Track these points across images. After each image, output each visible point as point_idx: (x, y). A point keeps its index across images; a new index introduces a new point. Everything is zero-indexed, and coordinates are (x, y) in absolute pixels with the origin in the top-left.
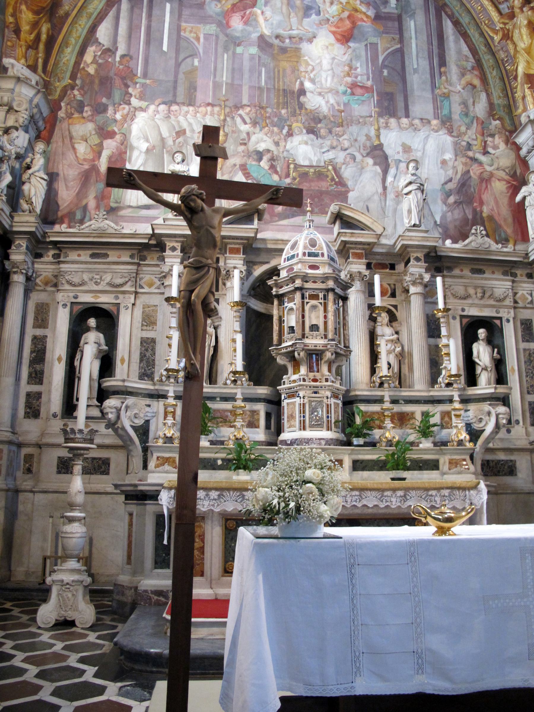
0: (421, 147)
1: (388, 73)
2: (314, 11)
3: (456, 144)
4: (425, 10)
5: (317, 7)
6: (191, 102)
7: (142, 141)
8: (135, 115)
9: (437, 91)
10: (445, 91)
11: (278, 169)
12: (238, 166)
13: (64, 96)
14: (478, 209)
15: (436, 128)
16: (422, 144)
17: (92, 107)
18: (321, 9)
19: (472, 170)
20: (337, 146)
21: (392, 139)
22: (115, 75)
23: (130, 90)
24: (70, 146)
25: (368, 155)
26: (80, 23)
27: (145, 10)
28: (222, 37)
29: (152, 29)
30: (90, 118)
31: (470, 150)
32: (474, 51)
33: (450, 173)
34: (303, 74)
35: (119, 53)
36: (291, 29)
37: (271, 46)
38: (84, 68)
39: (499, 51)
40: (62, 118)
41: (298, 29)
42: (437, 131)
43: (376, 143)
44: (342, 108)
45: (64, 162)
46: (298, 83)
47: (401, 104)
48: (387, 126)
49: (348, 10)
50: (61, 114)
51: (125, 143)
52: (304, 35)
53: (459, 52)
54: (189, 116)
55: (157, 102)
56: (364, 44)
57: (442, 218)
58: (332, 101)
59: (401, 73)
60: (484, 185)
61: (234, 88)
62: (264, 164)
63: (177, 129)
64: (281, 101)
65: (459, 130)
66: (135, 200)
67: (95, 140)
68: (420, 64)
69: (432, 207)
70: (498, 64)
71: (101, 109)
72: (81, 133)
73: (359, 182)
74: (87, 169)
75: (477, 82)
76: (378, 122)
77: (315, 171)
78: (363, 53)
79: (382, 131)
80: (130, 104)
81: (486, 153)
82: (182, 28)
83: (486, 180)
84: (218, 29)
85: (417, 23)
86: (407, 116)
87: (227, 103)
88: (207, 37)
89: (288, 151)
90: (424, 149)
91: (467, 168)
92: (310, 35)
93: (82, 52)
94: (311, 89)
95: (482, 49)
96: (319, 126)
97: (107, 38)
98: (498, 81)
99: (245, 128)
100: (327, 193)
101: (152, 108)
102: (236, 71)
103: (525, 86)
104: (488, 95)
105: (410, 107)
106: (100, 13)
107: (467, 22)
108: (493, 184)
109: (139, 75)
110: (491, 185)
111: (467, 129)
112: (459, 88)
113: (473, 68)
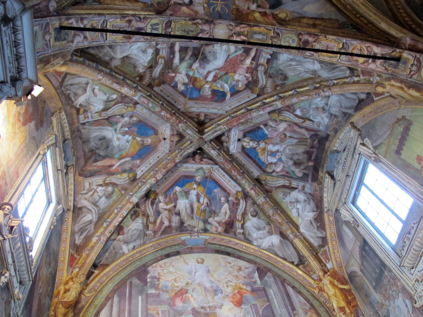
26: (90, 311)
28: (172, 312)
29: (132, 311)
32: (307, 300)
36: (209, 303)
39: (319, 297)
41: (212, 302)
53: (300, 302)
56: (249, 305)
70: (322, 304)
78: (250, 310)
84: (169, 307)
88: (163, 312)
92: (220, 305)
95: (311, 298)
98: (325, 313)
113: (310, 309)
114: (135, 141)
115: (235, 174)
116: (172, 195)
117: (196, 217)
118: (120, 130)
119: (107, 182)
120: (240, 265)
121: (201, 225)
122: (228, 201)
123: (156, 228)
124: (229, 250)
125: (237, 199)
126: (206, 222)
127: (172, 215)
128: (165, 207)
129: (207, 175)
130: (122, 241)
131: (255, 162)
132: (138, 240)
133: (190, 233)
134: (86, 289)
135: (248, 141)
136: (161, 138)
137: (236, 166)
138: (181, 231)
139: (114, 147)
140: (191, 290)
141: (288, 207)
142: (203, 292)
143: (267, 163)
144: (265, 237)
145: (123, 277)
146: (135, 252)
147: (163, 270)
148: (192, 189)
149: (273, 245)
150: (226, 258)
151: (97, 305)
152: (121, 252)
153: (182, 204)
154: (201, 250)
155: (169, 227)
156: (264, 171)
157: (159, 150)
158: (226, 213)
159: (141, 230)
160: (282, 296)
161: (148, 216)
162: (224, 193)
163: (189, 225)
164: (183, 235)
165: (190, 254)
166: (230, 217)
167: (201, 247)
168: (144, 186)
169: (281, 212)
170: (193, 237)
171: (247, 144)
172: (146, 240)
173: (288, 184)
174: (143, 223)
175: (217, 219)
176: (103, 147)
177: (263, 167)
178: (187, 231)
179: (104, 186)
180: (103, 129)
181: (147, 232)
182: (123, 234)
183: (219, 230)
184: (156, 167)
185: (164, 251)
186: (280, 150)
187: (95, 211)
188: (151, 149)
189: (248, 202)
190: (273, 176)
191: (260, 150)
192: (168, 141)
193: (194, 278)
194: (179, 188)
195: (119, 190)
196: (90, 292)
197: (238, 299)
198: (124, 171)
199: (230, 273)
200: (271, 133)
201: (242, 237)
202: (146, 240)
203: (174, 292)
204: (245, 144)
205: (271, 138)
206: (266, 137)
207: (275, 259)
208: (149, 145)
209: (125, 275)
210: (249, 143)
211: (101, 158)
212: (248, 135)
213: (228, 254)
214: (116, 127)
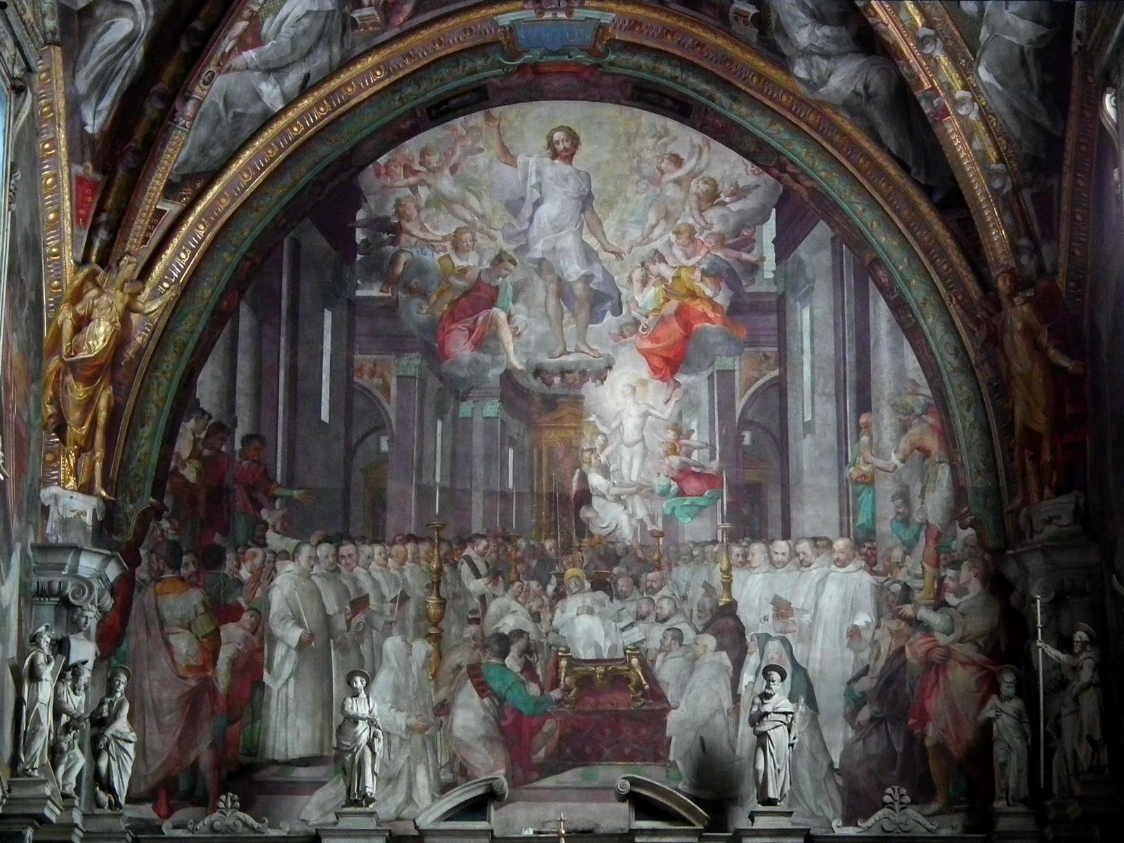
0: (811, 601)
1: (753, 440)
2: (609, 304)
3: (880, 590)
4: (834, 279)
5: (616, 296)
6: (377, 536)
7: (290, 624)
8: (275, 569)
9: (851, 471)
10: (865, 468)
11: (539, 671)
12: (464, 670)
13: (145, 535)
14: (917, 731)
15: (842, 557)
16: (812, 595)
17: (196, 556)
18: (623, 298)
19: (910, 645)
20: (648, 613)
21: (754, 591)
22: (235, 481)
23: (264, 514)
24: (160, 640)
25: (707, 628)
27: (283, 329)
28: (434, 384)
30: (194, 579)
31: (910, 602)
33: (865, 655)
34: (587, 455)
35: (240, 432)
37: (524, 393)
38: (176, 469)
40: (143, 581)
41: (578, 351)
42: (843, 565)
43: (724, 600)
44: (660, 527)
45: (153, 674)
46: (576, 476)
47: (775, 509)
48: (745, 562)
49: (675, 295)
50: (141, 573)
51: (260, 630)
52: (589, 364)
53: (900, 374)
54: (373, 566)
55: (314, 539)
56: (705, 374)
57: (842, 754)
58: (641, 513)
59: (778, 437)
60: (932, 674)
61: (456, 499)
62: (512, 662)
63: (353, 596)
64: (544, 520)
65: (889, 559)
66: (283, 750)
67: (204, 627)
68: (818, 410)
69: (825, 734)
71: (211, 559)
72: (179, 614)
73: (688, 686)
74: (194, 688)
75: (932, 443)
76: (729, 554)
77: (607, 671)
78: (704, 396)
79: (734, 573)
80: (264, 545)
81: (939, 604)
82: (356, 366)
83: (935, 665)
85: (815, 312)
86: (786, 536)
87: (444, 533)
89: (556, 631)
90: (816, 605)
91: (901, 643)
92: (602, 364)
93: (170, 438)
94: (603, 490)
96: (615, 570)
97: (215, 399)
99: (476, 586)
100: (631, 716)
101: (306, 550)
102: (457, 460)
103: (1027, 452)
104: (953, 468)
105: (794, 514)
106: (199, 341)
107: (920, 300)
108: (950, 675)
109: (279, 479)
110: (946, 677)
111: (905, 553)
112: (895, 459)
120: (715, 174)
124: (694, 86)
132: (319, 51)
134: (144, 289)
140: (510, 289)
142: (552, 302)
145: (267, 220)
146: (306, 102)
150: (667, 132)
151: (185, 345)
152: (256, 109)
160: (840, 343)
167: (577, 64)
170: (548, 15)
172: (353, 43)
181: (356, 15)
185: (425, 85)
193: (526, 232)
196: (154, 296)
197: (670, 341)
199: (667, 216)
201: (752, 33)
202: (353, 43)
203: (449, 297)
207: (869, 157)
213: (681, 109)
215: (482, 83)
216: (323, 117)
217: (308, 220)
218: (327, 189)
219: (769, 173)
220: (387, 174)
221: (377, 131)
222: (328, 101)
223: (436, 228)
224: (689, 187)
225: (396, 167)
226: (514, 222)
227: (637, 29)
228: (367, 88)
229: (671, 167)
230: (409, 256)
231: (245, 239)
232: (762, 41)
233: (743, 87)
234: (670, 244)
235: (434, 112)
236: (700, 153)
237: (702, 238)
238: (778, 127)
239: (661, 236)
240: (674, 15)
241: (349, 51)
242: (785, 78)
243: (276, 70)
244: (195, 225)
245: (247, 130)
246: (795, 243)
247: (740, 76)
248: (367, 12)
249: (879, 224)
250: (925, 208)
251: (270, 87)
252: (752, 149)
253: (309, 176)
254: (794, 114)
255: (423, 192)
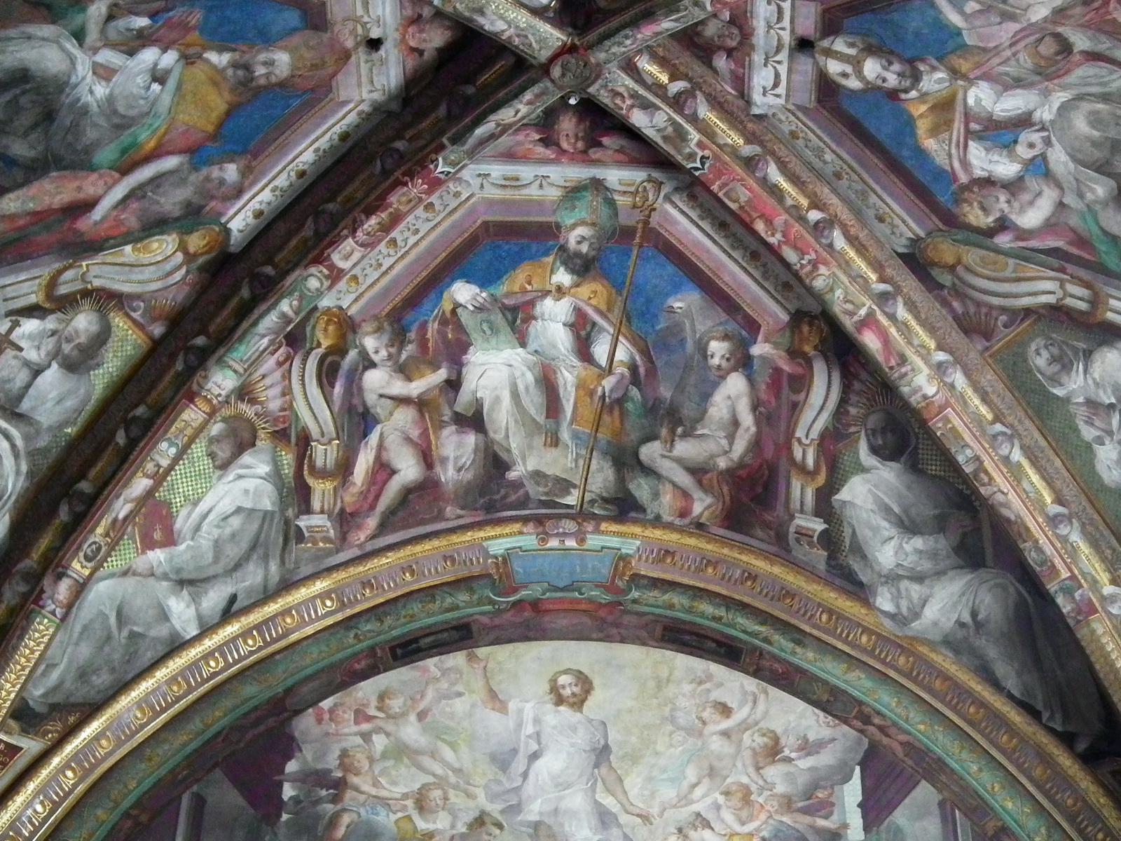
114: (198, 71)
115: (772, 240)
116: (432, 328)
117: (575, 436)
118: (103, 31)
119: (63, 290)
120: (777, 725)
121: (602, 477)
122: (743, 362)
123: (348, 499)
124: (742, 627)
125: (794, 353)
126: (626, 460)
127: (441, 425)
128: (399, 387)
129: (626, 219)
130: (165, 577)
131: (895, 166)
132: (251, 567)
133: (539, 520)
135: (852, 51)
136: (349, 44)
137: (785, 185)
138: (490, 508)
139: (85, 111)
141: (1076, 430)
143: (963, 178)
144: (939, 574)
145: (163, 771)
147: (366, 737)
148: (546, 293)
149: (978, 625)
150: (709, 677)
152: (161, 631)
153: (494, 370)
154: (586, 620)
155: (426, 489)
156: (951, 221)
157: (344, 103)
158: (736, 423)
159: (267, 515)
161: (305, 441)
162: (724, 316)
163: (538, 475)
164: (498, 530)
165: (521, 647)
166: (756, 445)
167: (590, 601)
168: (263, 307)
169: (1026, 450)
170: (554, 543)
171: (849, 69)
173: (1083, 306)
174: (276, 476)
175: (684, 448)
176: (25, 120)
177: (943, 199)
178: (524, 502)
179: (52, 312)
180: (10, 39)
181: (303, 522)
182: (170, 540)
183: (697, 508)
184: (332, 199)
185: (389, 621)
186: (1037, 116)
187: (13, 446)
188: (296, 103)
189: (856, 376)
190: (998, 251)
191: (923, 108)
192: (390, 52)
193: (517, 790)
194: (475, 289)
195: (134, 321)
198: (156, 225)
199: (712, 773)
200: (978, 23)
201: (819, 556)
204: (834, 67)
205: (985, 50)
206: (951, 45)
207: (982, 704)
208: (282, 84)
209: (179, 758)
210: (857, 64)
211: (19, 175)
212: (847, 23)
213: (729, 652)
214: (78, 19)
215: (466, 620)
216: (251, 653)
217: (218, 774)
218: (249, 736)
219: (850, 726)
220: (331, 719)
221: (322, 670)
222: (259, 632)
223: (394, 783)
224: (741, 740)
225: (344, 712)
226: (504, 780)
227: (669, 560)
228: (312, 621)
229: (717, 717)
230: (355, 816)
231: (130, 792)
232: (834, 568)
233: (807, 629)
234: (718, 808)
235: (399, 651)
236: (755, 702)
237: (761, 800)
238: (857, 673)
239: (704, 796)
240: (716, 541)
241: (291, 572)
242: (864, 611)
243: (191, 582)
244: (61, 770)
245: (148, 656)
246: (892, 806)
247: (804, 615)
248: (318, 520)
249: (1003, 787)
250: (1065, 761)
251: (182, 605)
252: (825, 697)
253: (225, 722)
254: (877, 658)
255: (379, 742)
